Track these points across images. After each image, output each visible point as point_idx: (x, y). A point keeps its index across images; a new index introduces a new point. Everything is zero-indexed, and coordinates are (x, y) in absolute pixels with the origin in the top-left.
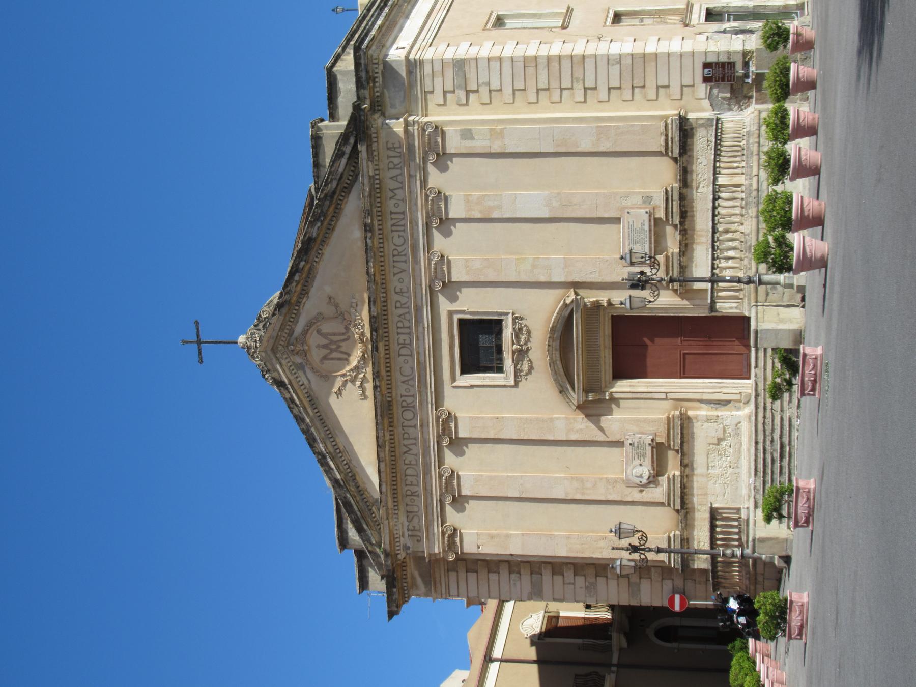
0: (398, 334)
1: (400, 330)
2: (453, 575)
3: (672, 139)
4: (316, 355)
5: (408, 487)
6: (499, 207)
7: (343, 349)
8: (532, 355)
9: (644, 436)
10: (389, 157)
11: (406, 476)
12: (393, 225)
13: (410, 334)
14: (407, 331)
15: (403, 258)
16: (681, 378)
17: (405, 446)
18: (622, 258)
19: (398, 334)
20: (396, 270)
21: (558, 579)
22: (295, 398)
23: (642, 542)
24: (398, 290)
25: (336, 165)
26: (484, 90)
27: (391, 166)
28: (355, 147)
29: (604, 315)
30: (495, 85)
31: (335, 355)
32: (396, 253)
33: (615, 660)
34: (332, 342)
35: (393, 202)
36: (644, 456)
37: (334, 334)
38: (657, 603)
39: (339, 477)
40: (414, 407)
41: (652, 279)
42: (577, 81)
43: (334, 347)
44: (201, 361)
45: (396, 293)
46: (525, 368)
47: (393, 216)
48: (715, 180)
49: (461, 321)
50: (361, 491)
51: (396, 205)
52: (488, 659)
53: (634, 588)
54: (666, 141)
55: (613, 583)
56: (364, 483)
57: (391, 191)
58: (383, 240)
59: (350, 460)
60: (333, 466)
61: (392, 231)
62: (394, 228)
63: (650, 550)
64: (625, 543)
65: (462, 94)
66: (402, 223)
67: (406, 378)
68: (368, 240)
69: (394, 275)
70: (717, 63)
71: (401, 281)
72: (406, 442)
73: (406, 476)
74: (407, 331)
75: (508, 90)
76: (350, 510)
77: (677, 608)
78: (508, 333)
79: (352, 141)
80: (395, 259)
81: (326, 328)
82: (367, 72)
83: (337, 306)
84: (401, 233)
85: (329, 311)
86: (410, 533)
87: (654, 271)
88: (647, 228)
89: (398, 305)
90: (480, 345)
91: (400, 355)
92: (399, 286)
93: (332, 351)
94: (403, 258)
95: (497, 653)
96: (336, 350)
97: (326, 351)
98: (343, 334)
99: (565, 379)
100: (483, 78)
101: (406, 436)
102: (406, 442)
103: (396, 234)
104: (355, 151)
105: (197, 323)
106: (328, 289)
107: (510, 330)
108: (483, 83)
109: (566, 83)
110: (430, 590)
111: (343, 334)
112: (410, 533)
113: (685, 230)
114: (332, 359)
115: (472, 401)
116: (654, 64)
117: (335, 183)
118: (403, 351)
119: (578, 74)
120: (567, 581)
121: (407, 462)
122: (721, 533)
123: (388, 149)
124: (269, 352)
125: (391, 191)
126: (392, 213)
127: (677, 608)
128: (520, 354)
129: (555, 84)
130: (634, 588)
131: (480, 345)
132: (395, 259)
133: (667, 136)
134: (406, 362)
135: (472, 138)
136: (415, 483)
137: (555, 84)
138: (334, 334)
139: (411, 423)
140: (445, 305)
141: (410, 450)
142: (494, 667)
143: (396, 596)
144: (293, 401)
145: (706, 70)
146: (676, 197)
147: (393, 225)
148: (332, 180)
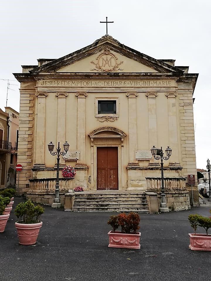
1: (112, 82)
2: (28, 95)
3: (175, 166)
4: (104, 57)
5: (60, 82)
10: (166, 82)
16: (98, 169)
18: (168, 147)
20: (132, 82)
21: (27, 129)
22: (91, 48)
23: (62, 153)
25: (166, 65)
26: (184, 111)
27: (164, 82)
28: (171, 71)
29: (118, 144)
30: (185, 114)
31: (104, 62)
32: (137, 82)
34: (109, 61)
37: (111, 63)
39: (65, 60)
40: (88, 85)
41: (162, 157)
44: (101, 22)
45: (124, 82)
47: (148, 82)
49: (115, 102)
50: (59, 67)
53: (24, 154)
54: (174, 164)
56: (62, 68)
58: (142, 79)
59: (69, 65)
60: (69, 58)
61: (144, 82)
62: (145, 82)
63: (58, 156)
64: (62, 147)
66: (146, 85)
67: (97, 83)
68: (142, 74)
69: (130, 82)
75: (184, 118)
76: (53, 63)
78: (112, 115)
79: (173, 70)
80: (135, 82)
81: (113, 60)
82: (190, 77)
84: (143, 84)
85: (119, 62)
89: (121, 82)
90: (107, 107)
91: (105, 82)
96: (106, 63)
98: (111, 65)
101: (78, 82)
104: (170, 71)
105: (113, 22)
109: (186, 135)
110: (22, 87)
111: (111, 65)
113: (147, 170)
114: (103, 61)
115: (91, 103)
117: (160, 65)
119: (189, 139)
122: (158, 186)
123: (169, 82)
124: (106, 41)
125: (156, 82)
126: (149, 82)
128: (107, 119)
130: (24, 154)
131: (107, 107)
132: (135, 82)
133: (175, 164)
135: (172, 107)
137: (186, 132)
140: (123, 95)
143: (21, 76)
144: (90, 47)
145: (192, 176)
146: (157, 167)
148: (161, 64)
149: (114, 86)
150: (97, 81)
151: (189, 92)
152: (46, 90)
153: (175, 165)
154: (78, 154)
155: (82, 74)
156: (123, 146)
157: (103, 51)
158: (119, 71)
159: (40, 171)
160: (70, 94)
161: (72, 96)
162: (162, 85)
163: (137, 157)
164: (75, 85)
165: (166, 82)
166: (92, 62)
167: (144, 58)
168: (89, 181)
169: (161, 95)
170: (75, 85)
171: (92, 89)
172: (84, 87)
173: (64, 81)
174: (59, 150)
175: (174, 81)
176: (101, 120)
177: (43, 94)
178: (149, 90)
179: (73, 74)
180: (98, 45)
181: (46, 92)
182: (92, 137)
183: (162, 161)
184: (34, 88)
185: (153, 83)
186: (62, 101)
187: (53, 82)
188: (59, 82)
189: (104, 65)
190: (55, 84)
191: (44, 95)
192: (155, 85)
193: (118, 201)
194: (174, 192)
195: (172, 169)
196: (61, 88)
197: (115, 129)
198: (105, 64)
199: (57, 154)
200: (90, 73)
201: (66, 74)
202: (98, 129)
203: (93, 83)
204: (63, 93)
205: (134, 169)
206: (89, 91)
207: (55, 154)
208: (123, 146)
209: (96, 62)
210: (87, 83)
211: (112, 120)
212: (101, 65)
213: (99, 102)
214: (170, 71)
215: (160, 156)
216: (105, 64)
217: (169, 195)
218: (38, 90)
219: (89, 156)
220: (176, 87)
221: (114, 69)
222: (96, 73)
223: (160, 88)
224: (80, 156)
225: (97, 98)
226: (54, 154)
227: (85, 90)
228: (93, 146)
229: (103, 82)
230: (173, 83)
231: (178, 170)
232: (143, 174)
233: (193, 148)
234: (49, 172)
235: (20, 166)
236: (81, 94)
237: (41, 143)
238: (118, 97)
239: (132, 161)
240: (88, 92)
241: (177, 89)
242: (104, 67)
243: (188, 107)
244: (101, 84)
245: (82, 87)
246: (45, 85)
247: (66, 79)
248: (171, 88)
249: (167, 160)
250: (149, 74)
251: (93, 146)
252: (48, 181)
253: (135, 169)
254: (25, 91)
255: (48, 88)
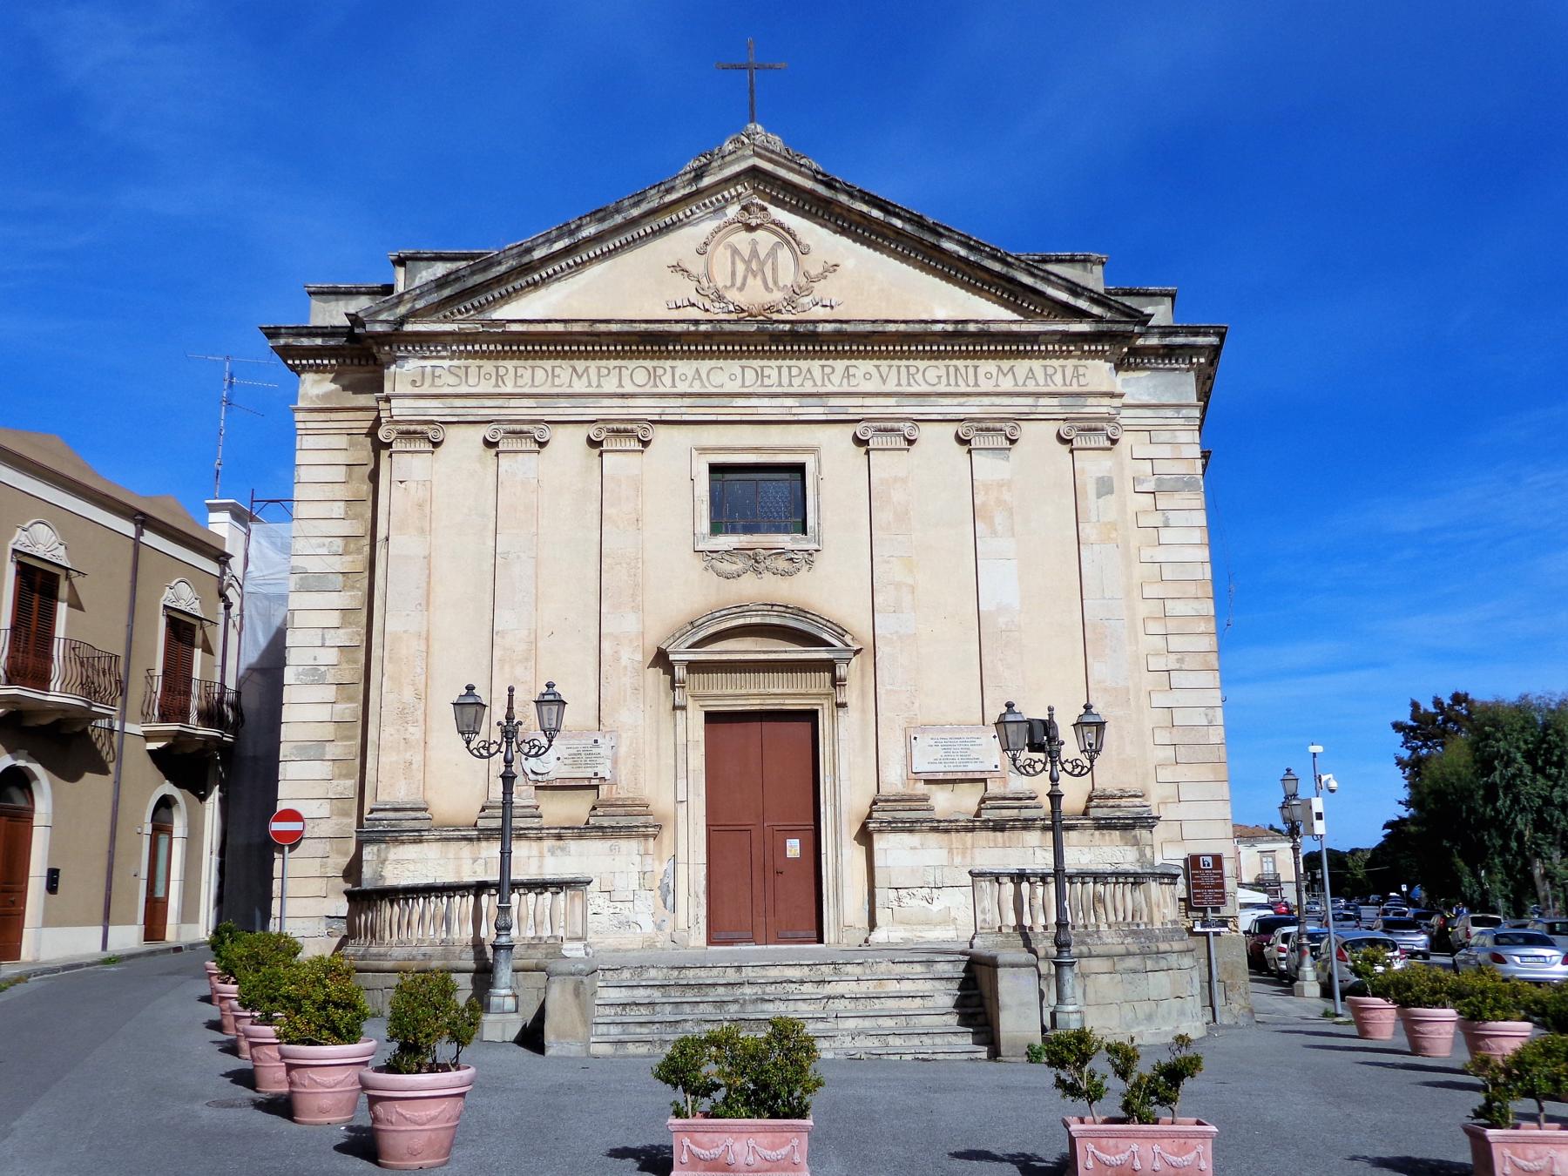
0: (780, 368)
1: (785, 371)
4: (742, 239)
5: (511, 371)
6: (994, 533)
7: (750, 280)
8: (749, 578)
9: (608, 763)
10: (1063, 367)
11: (533, 368)
12: (957, 369)
13: (780, 385)
14: (785, 380)
15: (904, 381)
17: (587, 369)
19: (780, 368)
20: (884, 370)
21: (334, 619)
23: (526, 748)
24: (852, 371)
26: (1157, 519)
27: (1050, 371)
30: (1167, 535)
31: (740, 267)
32: (913, 370)
33: (129, 728)
34: (762, 264)
35: (994, 371)
36: (575, 764)
37: (774, 270)
38: (283, 790)
42: (1178, 660)
43: (754, 266)
46: (726, 567)
47: (971, 371)
48: (1154, 876)
49: (800, 469)
51: (988, 376)
52: (144, 521)
54: (1113, 797)
55: (324, 713)
57: (1012, 368)
59: (558, 279)
61: (947, 367)
62: (952, 370)
63: (508, 762)
65: (1150, 486)
66: (960, 381)
67: (704, 376)
69: (877, 367)
70: (1222, 875)
71: (868, 376)
72: (593, 371)
73: (533, 368)
74: (785, 380)
75: (1160, 554)
77: (276, 826)
78: (784, 541)
80: (903, 370)
81: (785, 255)
82: (1182, 346)
83: (822, 276)
84: (944, 380)
85: (813, 266)
86: (429, 369)
87: (1068, 767)
88: (971, 767)
90: (758, 497)
91: (743, 368)
92: (859, 373)
93: (748, 263)
94: (904, 381)
95: (149, 538)
96: (748, 269)
97: (746, 253)
98: (775, 283)
99: (712, 630)
100: (1174, 518)
102: (593, 371)
103: (943, 372)
104: (1081, 315)
106: (848, 264)
107: (790, 546)
108: (1167, 519)
109: (1176, 643)
111: (775, 283)
112: (429, 369)
113: (973, 830)
114: (733, 263)
116: (1212, 778)
118: (750, 374)
120: (330, 634)
121: (557, 371)
123: (1076, 367)
125: (1012, 368)
126: (976, 367)
127: (276, 826)
128: (755, 560)
129: (1172, 626)
130: (313, 750)
131: (758, 497)
132: (903, 370)
134: (732, 377)
135: (1099, 496)
136: (520, 382)
137: (1172, 626)
138: (774, 270)
139: (626, 381)
141: (580, 377)
142: (129, 528)
145: (1209, 859)
146: (1026, 814)
147: (957, 369)
149: (791, 390)
150: (705, 365)
151: (1181, 421)
152: (433, 409)
153: (1117, 802)
154: (605, 749)
155: (626, 328)
156: (843, 705)
157: (733, 211)
158: (819, 313)
159: (403, 842)
160: (560, 429)
161: (568, 443)
162: (1042, 382)
163: (921, 765)
164: (590, 385)
165: (1063, 367)
166: (678, 268)
167: (947, 245)
168: (668, 893)
169: (1038, 437)
170: (590, 385)
171: (679, 402)
172: (633, 396)
173: (530, 362)
174: (509, 731)
175: (1099, 363)
176: (726, 567)
177: (426, 436)
178: (973, 408)
179: (577, 328)
180: (706, 181)
181: (432, 422)
182: (677, 657)
183: (1054, 781)
184: (374, 404)
185: (989, 373)
186: (519, 466)
187: (473, 371)
188: (502, 371)
189: (739, 282)
190: (481, 376)
191: (422, 436)
192: (1007, 384)
193: (829, 998)
194: (1121, 949)
195: (1104, 825)
196: (513, 402)
197: (801, 612)
198: (745, 278)
199: (503, 749)
200: (669, 321)
201: (540, 328)
202: (712, 617)
203: (684, 374)
204: (525, 428)
205: (902, 830)
206: (664, 418)
207: (493, 748)
208: (843, 705)
209: (696, 265)
210: (653, 375)
211: (782, 564)
212: (721, 280)
213: (715, 469)
214: (1081, 315)
215: (1041, 756)
216: (745, 278)
217: (1095, 965)
218: (400, 408)
219: (660, 755)
220: (1112, 395)
221: (790, 301)
222: (696, 322)
223: (1030, 401)
224: (615, 762)
225: (703, 450)
226: (485, 753)
227: (645, 408)
228: (684, 708)
229: (734, 366)
230: (1098, 373)
231: (1133, 827)
232: (950, 850)
233: (1210, 712)
234: (453, 846)
235: (293, 815)
236: (618, 431)
237: (408, 695)
238: (814, 443)
239: (894, 780)
240: (656, 418)
241: (1117, 402)
242: (741, 289)
243: (1177, 495)
244: (725, 374)
245: (623, 396)
246: (433, 385)
247: (542, 355)
248: (1091, 401)
249: (1080, 775)
250: (972, 328)
251: (684, 708)
252: (477, 897)
253: (910, 827)
254: (322, 416)
255: (449, 402)
